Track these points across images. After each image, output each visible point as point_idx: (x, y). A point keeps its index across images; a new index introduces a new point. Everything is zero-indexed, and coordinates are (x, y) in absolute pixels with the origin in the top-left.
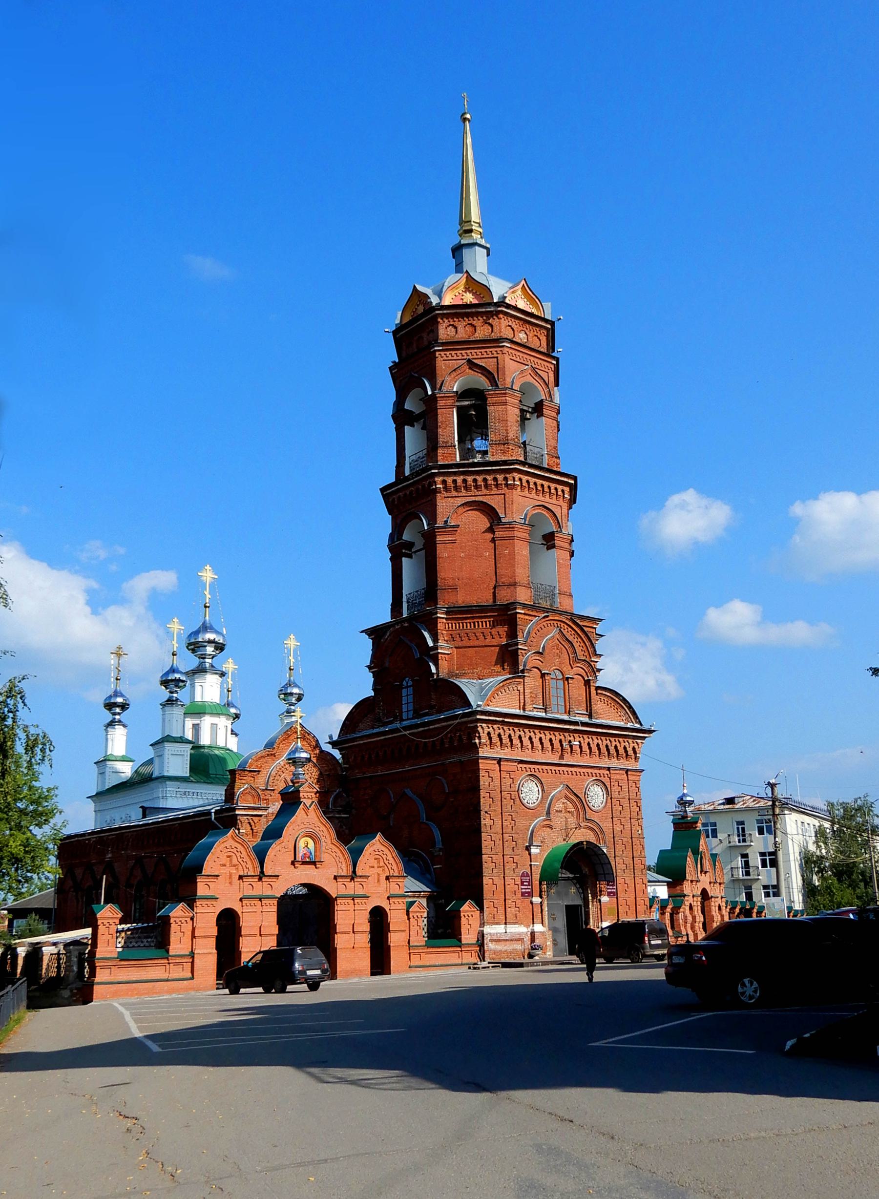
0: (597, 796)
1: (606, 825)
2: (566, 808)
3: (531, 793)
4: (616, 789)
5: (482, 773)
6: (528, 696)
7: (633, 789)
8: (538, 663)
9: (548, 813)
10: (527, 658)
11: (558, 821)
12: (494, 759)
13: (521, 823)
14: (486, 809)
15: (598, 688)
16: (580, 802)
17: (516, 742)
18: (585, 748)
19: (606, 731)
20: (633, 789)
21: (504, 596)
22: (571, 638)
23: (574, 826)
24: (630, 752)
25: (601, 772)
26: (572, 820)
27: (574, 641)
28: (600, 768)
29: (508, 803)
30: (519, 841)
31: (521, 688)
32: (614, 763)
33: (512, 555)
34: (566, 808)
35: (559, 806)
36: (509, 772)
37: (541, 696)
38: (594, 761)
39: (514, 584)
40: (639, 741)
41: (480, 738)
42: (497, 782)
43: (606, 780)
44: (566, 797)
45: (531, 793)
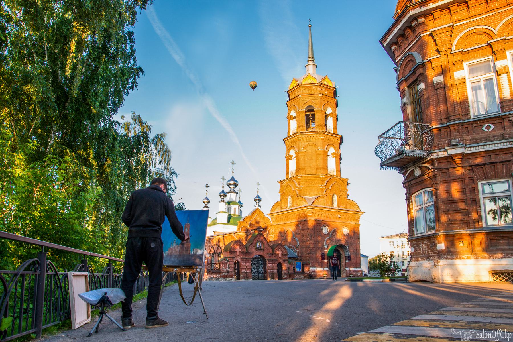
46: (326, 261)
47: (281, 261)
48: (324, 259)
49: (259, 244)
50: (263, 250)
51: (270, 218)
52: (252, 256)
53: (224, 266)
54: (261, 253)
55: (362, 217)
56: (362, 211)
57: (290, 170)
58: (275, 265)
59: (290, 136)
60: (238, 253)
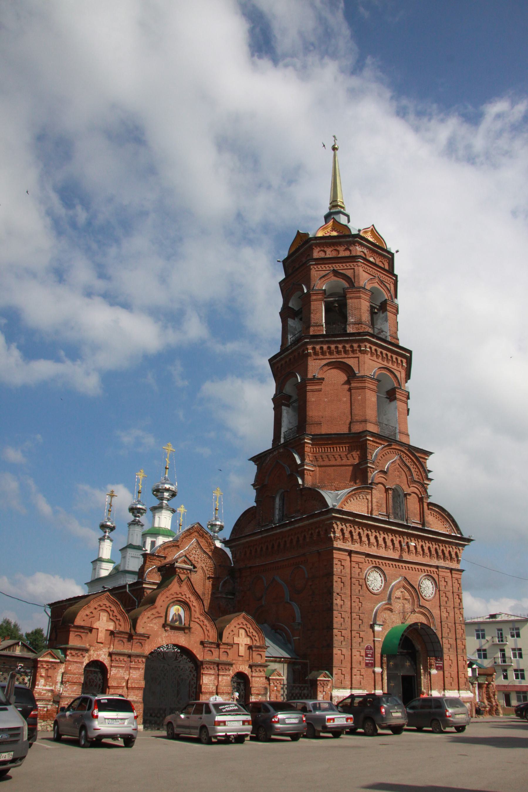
0: (428, 588)
1: (436, 612)
2: (403, 596)
3: (375, 581)
4: (443, 583)
5: (335, 561)
6: (374, 504)
7: (456, 585)
8: (382, 480)
9: (390, 598)
10: (374, 475)
11: (397, 606)
12: (345, 550)
13: (367, 605)
14: (338, 591)
15: (429, 504)
16: (415, 591)
17: (364, 539)
18: (419, 549)
19: (435, 538)
20: (456, 585)
21: (357, 428)
22: (408, 464)
23: (409, 610)
24: (454, 556)
25: (432, 569)
26: (408, 606)
27: (411, 467)
28: (431, 566)
29: (356, 588)
30: (365, 620)
31: (369, 497)
32: (441, 563)
33: (364, 400)
34: (403, 596)
35: (398, 593)
36: (357, 563)
37: (384, 506)
38: (426, 560)
39: (365, 421)
40: (460, 548)
41: (334, 532)
42: (348, 570)
43: (435, 576)
44: (404, 587)
45: (375, 581)
46: (378, 670)
47: (245, 669)
48: (373, 665)
49: (175, 610)
50: (184, 629)
51: (228, 551)
52: (148, 649)
53: (47, 677)
54: (182, 640)
55: (465, 553)
56: (466, 536)
57: (283, 430)
58: (226, 679)
59: (287, 349)
60: (102, 636)
